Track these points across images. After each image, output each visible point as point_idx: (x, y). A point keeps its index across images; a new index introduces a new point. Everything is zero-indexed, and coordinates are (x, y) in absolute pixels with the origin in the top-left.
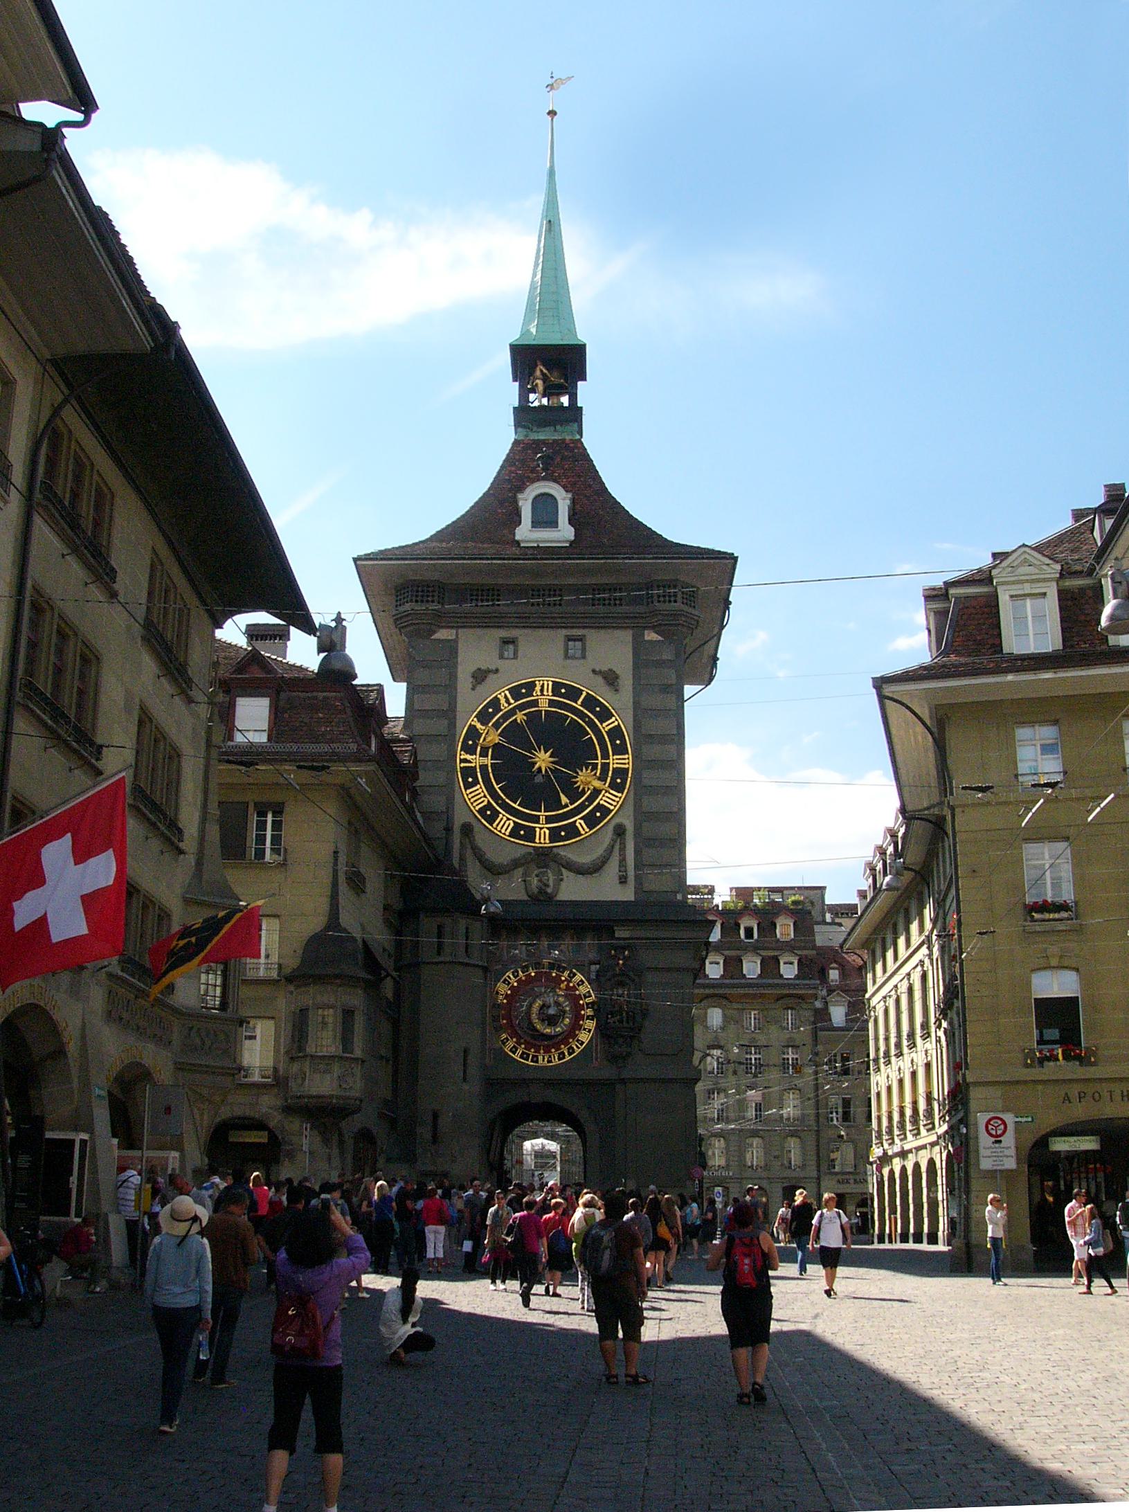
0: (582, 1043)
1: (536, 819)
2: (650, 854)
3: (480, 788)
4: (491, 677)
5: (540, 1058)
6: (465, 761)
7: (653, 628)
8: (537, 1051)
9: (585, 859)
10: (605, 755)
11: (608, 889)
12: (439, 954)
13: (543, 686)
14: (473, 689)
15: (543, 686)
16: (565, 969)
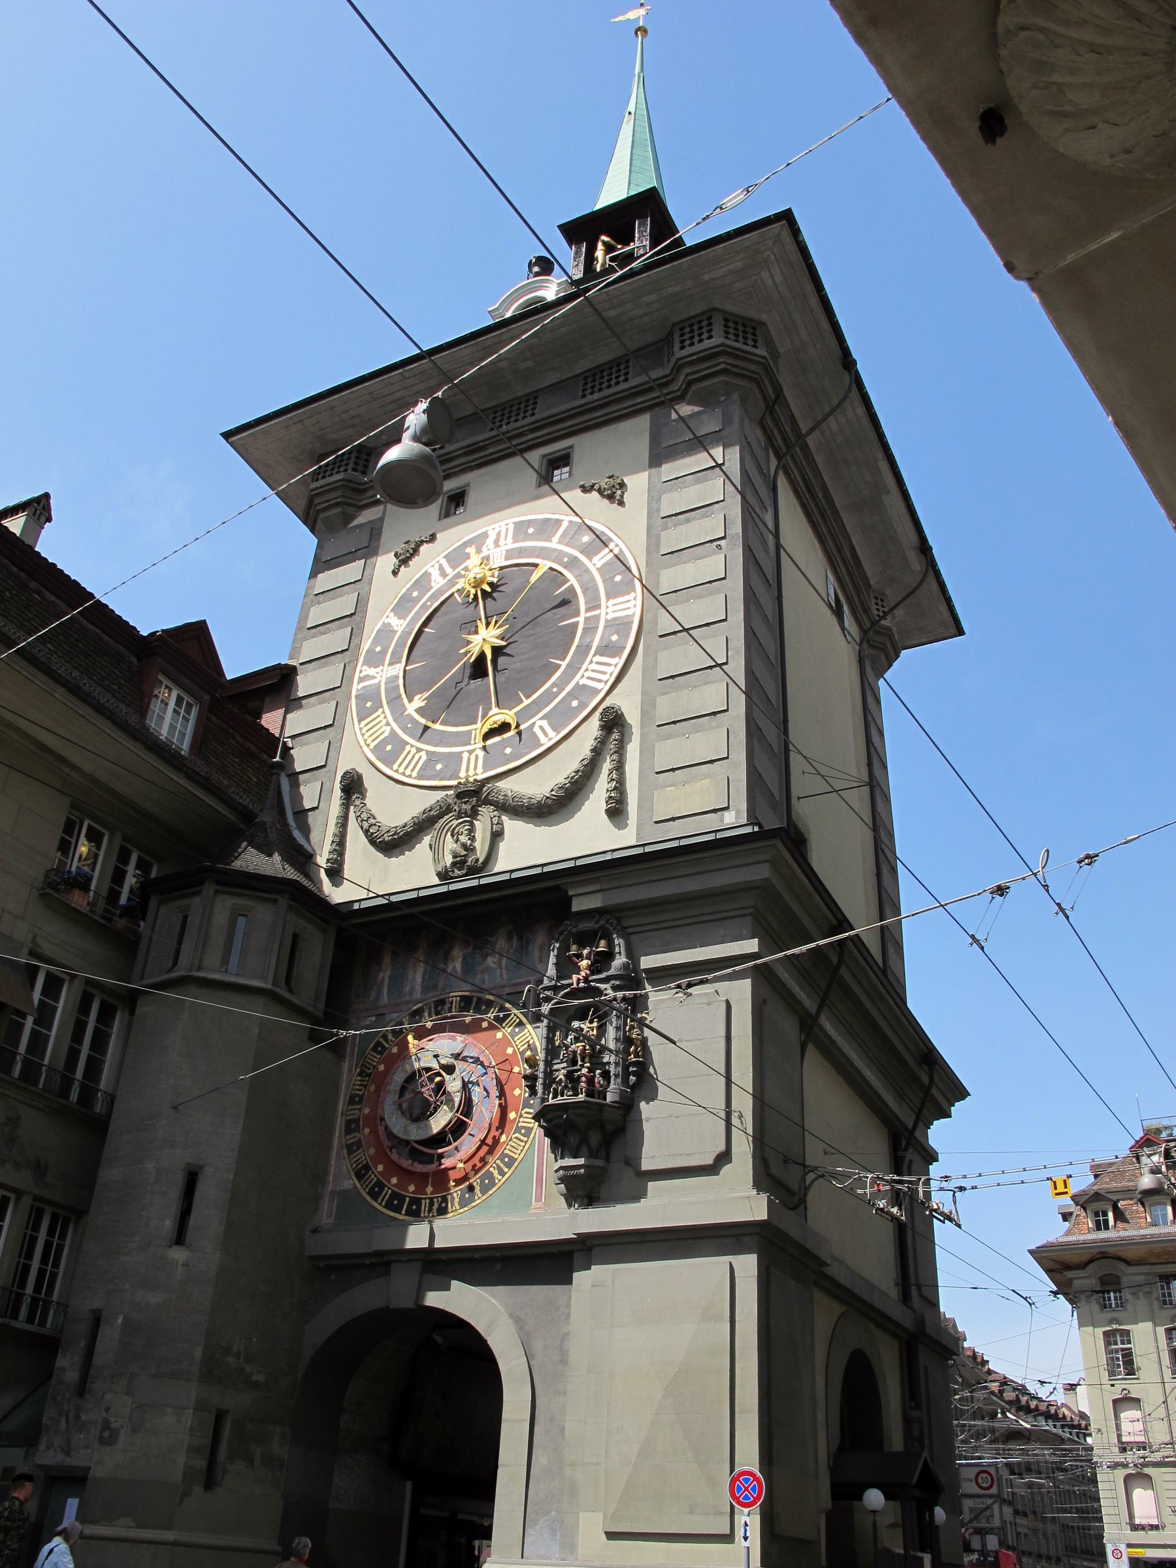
0: (512, 1160)
1: (465, 739)
2: (671, 752)
3: (385, 714)
4: (424, 548)
5: (425, 1204)
6: (367, 677)
7: (681, 398)
8: (421, 1189)
9: (536, 785)
10: (594, 605)
11: (587, 835)
12: (170, 970)
13: (499, 534)
14: (395, 573)
15: (499, 534)
16: (490, 1004)
